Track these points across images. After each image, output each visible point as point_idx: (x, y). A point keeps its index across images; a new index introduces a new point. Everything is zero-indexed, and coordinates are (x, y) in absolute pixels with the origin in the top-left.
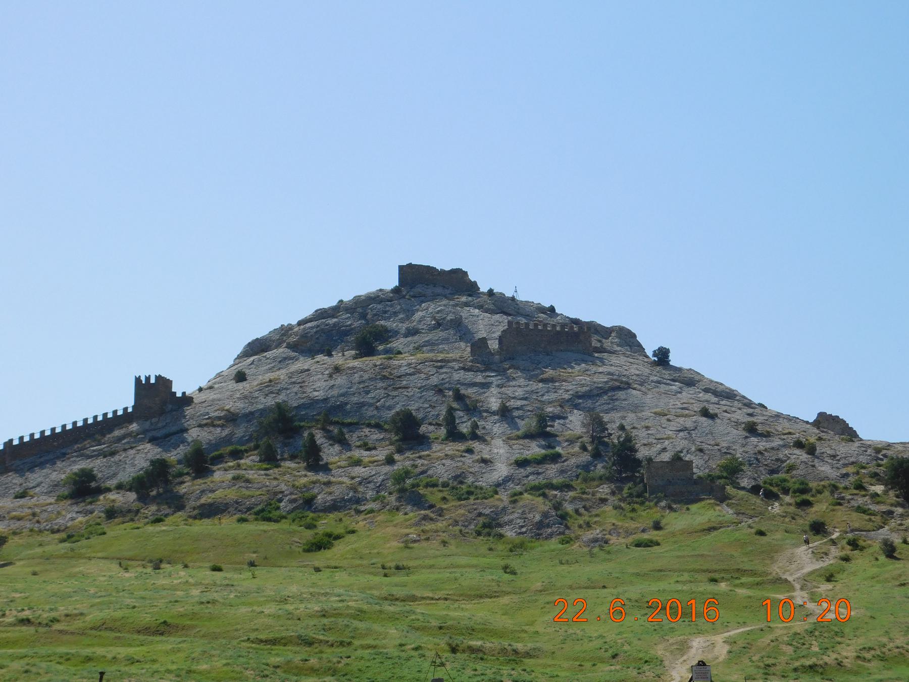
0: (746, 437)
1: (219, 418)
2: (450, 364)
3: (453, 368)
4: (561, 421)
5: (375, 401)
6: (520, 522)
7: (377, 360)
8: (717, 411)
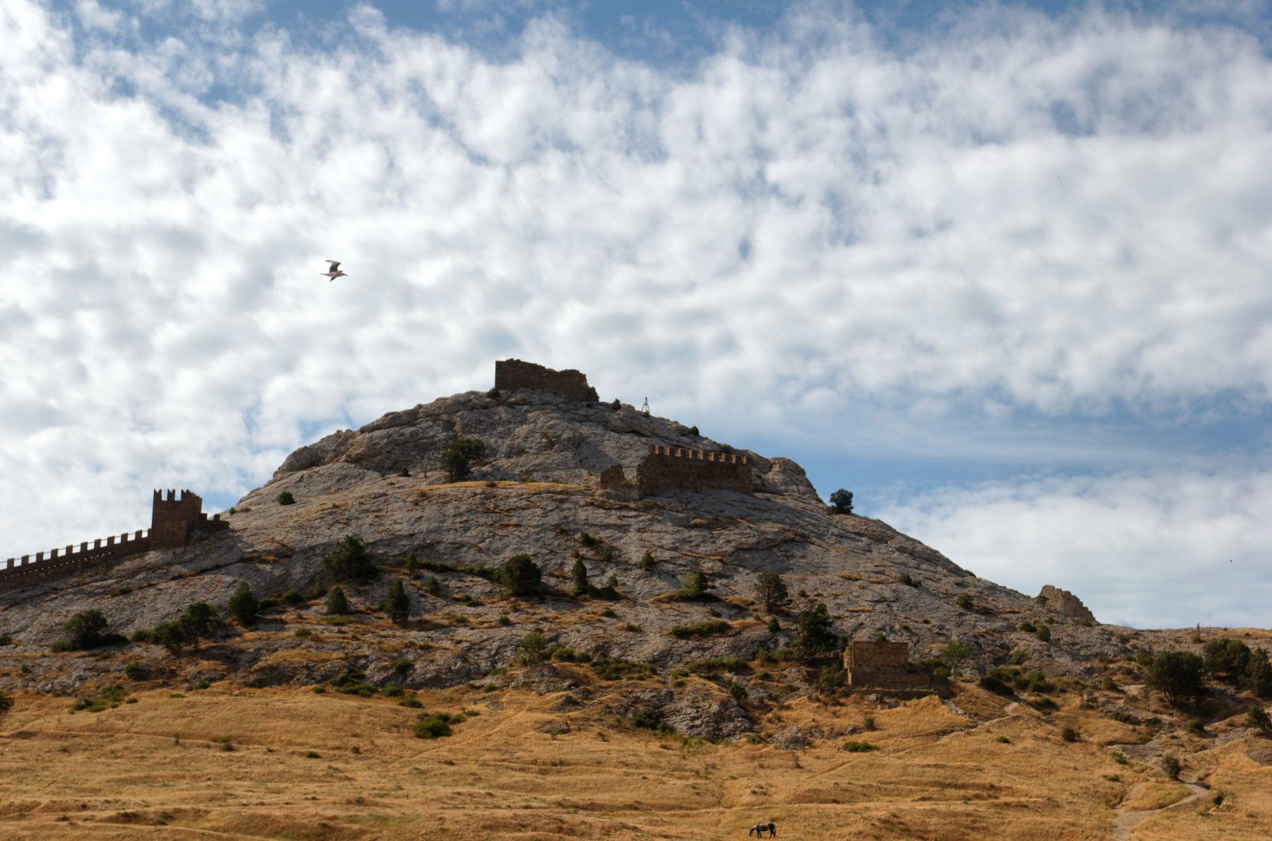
0: (961, 615)
1: (269, 552)
2: (573, 497)
3: (577, 503)
4: (724, 581)
5: (477, 541)
6: (693, 712)
7: (474, 486)
8: (919, 578)
